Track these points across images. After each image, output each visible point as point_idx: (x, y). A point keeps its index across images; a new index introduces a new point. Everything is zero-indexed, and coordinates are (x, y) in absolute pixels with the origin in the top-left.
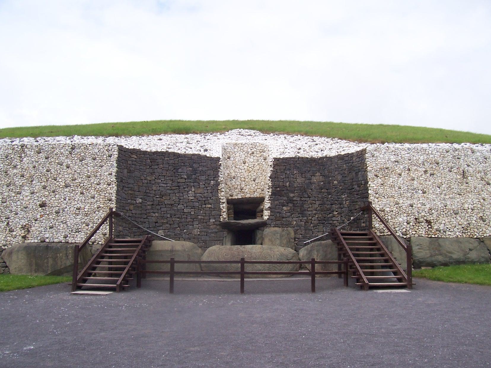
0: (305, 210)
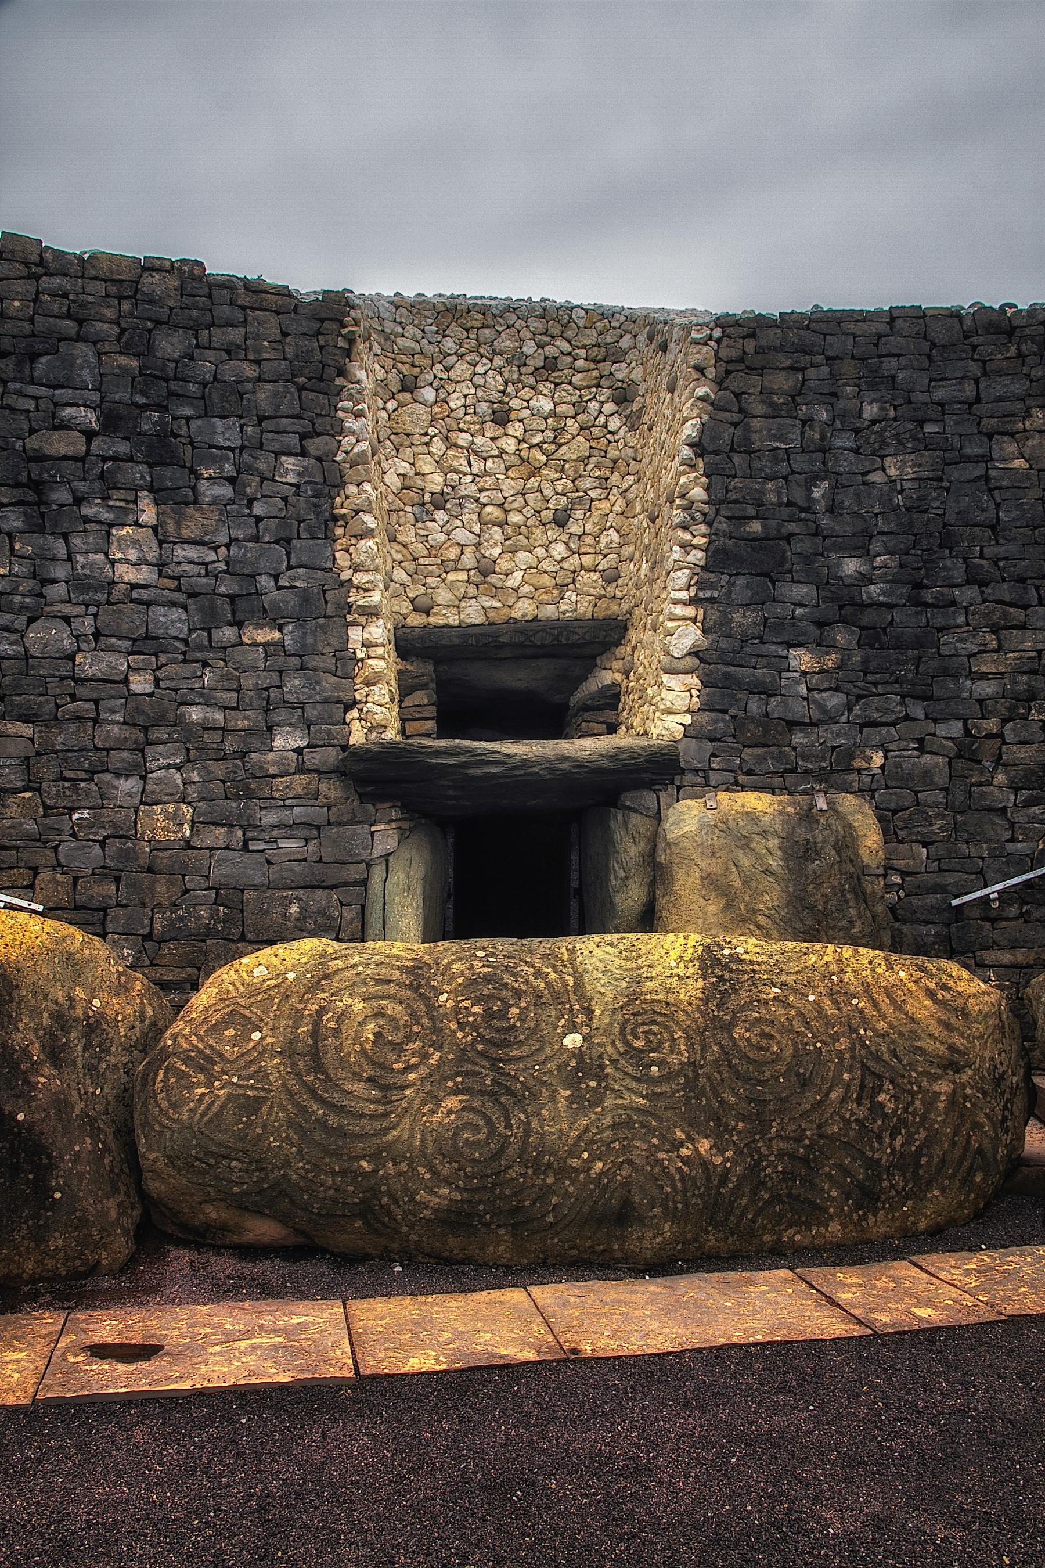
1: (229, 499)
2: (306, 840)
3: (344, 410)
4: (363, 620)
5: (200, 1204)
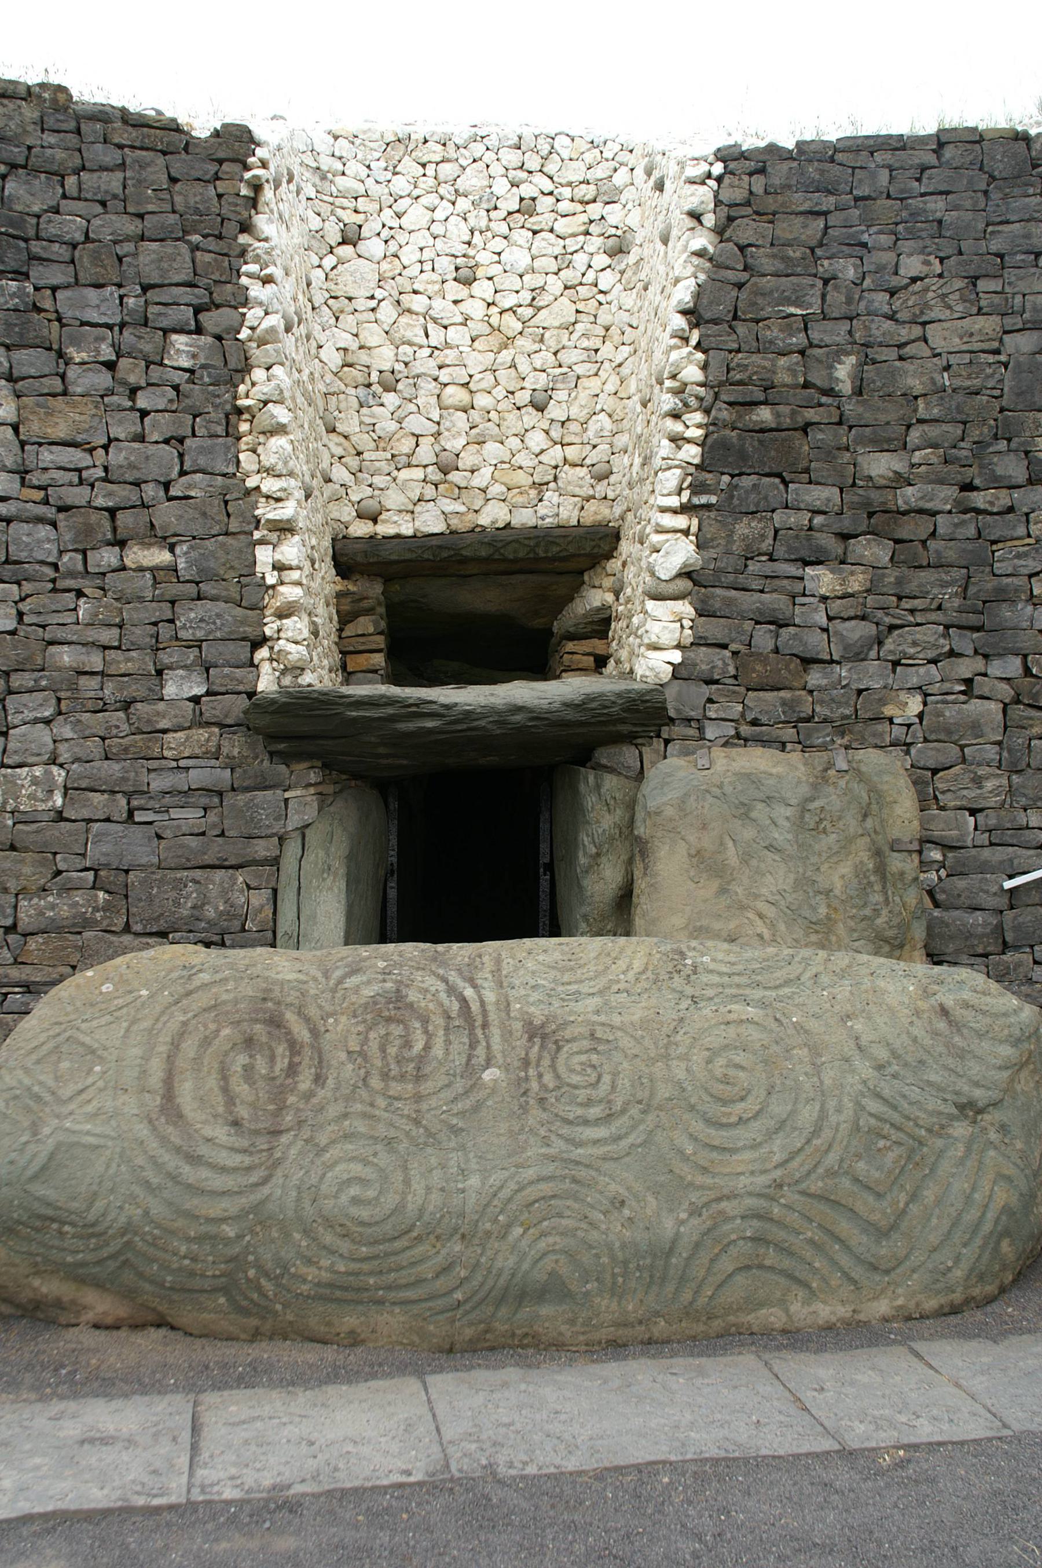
0: (1002, 597)
1: (107, 389)
2: (205, 809)
3: (249, 276)
4: (273, 537)
5: (27, 1276)
